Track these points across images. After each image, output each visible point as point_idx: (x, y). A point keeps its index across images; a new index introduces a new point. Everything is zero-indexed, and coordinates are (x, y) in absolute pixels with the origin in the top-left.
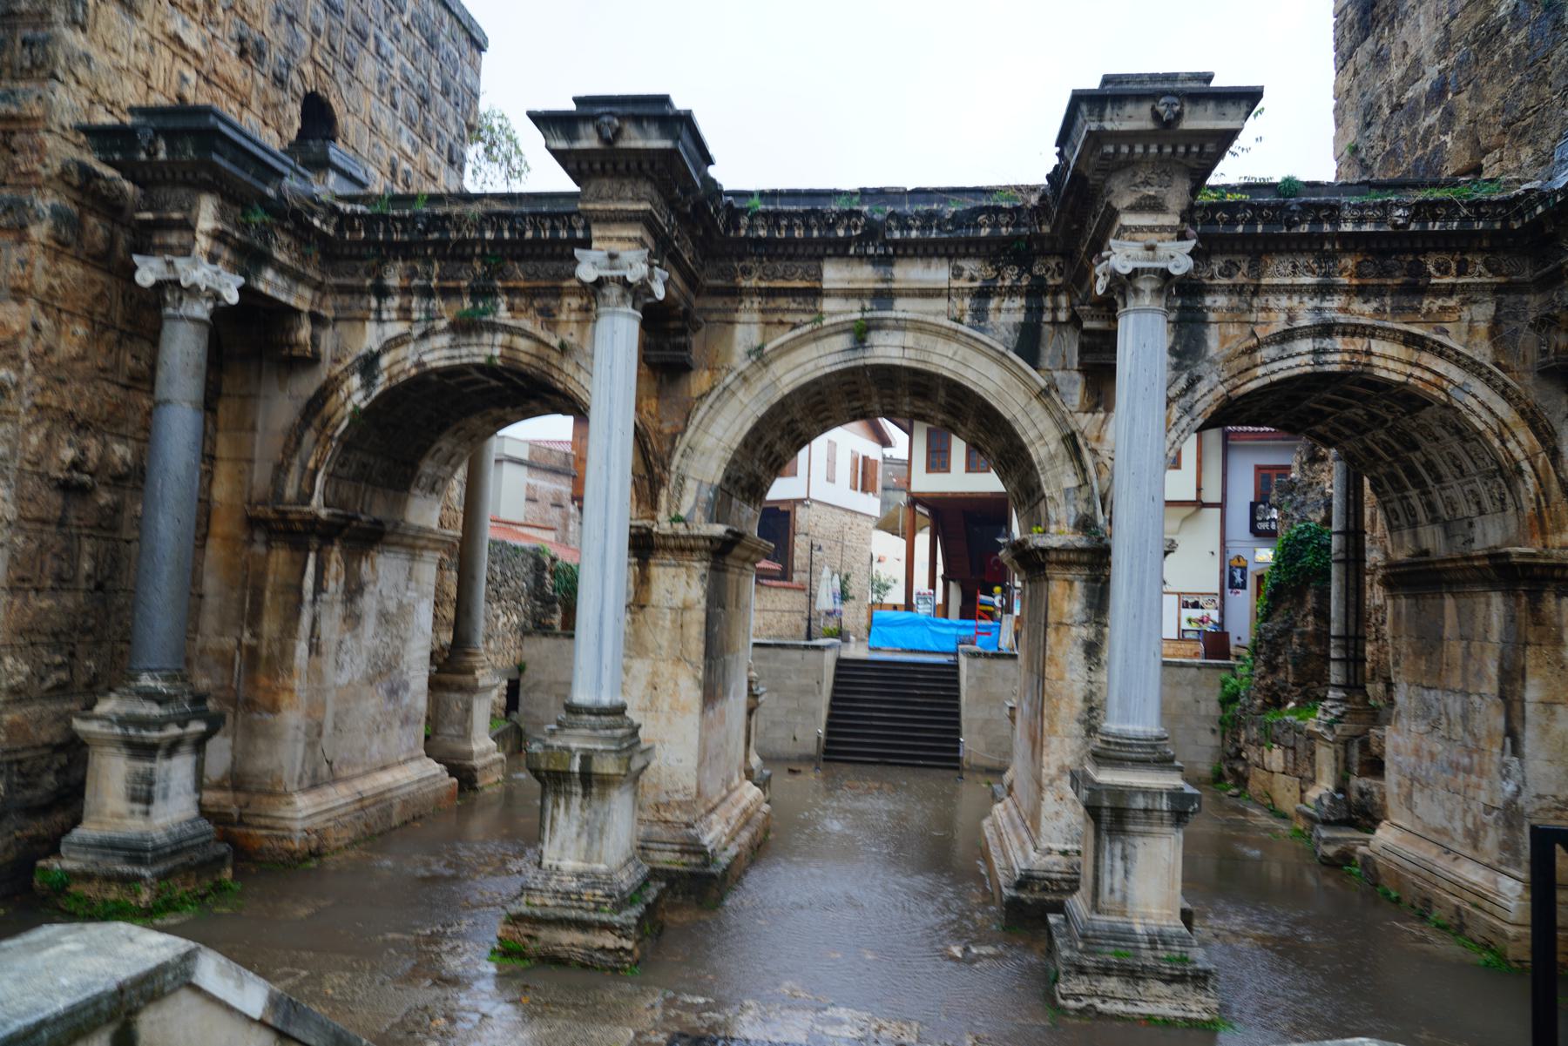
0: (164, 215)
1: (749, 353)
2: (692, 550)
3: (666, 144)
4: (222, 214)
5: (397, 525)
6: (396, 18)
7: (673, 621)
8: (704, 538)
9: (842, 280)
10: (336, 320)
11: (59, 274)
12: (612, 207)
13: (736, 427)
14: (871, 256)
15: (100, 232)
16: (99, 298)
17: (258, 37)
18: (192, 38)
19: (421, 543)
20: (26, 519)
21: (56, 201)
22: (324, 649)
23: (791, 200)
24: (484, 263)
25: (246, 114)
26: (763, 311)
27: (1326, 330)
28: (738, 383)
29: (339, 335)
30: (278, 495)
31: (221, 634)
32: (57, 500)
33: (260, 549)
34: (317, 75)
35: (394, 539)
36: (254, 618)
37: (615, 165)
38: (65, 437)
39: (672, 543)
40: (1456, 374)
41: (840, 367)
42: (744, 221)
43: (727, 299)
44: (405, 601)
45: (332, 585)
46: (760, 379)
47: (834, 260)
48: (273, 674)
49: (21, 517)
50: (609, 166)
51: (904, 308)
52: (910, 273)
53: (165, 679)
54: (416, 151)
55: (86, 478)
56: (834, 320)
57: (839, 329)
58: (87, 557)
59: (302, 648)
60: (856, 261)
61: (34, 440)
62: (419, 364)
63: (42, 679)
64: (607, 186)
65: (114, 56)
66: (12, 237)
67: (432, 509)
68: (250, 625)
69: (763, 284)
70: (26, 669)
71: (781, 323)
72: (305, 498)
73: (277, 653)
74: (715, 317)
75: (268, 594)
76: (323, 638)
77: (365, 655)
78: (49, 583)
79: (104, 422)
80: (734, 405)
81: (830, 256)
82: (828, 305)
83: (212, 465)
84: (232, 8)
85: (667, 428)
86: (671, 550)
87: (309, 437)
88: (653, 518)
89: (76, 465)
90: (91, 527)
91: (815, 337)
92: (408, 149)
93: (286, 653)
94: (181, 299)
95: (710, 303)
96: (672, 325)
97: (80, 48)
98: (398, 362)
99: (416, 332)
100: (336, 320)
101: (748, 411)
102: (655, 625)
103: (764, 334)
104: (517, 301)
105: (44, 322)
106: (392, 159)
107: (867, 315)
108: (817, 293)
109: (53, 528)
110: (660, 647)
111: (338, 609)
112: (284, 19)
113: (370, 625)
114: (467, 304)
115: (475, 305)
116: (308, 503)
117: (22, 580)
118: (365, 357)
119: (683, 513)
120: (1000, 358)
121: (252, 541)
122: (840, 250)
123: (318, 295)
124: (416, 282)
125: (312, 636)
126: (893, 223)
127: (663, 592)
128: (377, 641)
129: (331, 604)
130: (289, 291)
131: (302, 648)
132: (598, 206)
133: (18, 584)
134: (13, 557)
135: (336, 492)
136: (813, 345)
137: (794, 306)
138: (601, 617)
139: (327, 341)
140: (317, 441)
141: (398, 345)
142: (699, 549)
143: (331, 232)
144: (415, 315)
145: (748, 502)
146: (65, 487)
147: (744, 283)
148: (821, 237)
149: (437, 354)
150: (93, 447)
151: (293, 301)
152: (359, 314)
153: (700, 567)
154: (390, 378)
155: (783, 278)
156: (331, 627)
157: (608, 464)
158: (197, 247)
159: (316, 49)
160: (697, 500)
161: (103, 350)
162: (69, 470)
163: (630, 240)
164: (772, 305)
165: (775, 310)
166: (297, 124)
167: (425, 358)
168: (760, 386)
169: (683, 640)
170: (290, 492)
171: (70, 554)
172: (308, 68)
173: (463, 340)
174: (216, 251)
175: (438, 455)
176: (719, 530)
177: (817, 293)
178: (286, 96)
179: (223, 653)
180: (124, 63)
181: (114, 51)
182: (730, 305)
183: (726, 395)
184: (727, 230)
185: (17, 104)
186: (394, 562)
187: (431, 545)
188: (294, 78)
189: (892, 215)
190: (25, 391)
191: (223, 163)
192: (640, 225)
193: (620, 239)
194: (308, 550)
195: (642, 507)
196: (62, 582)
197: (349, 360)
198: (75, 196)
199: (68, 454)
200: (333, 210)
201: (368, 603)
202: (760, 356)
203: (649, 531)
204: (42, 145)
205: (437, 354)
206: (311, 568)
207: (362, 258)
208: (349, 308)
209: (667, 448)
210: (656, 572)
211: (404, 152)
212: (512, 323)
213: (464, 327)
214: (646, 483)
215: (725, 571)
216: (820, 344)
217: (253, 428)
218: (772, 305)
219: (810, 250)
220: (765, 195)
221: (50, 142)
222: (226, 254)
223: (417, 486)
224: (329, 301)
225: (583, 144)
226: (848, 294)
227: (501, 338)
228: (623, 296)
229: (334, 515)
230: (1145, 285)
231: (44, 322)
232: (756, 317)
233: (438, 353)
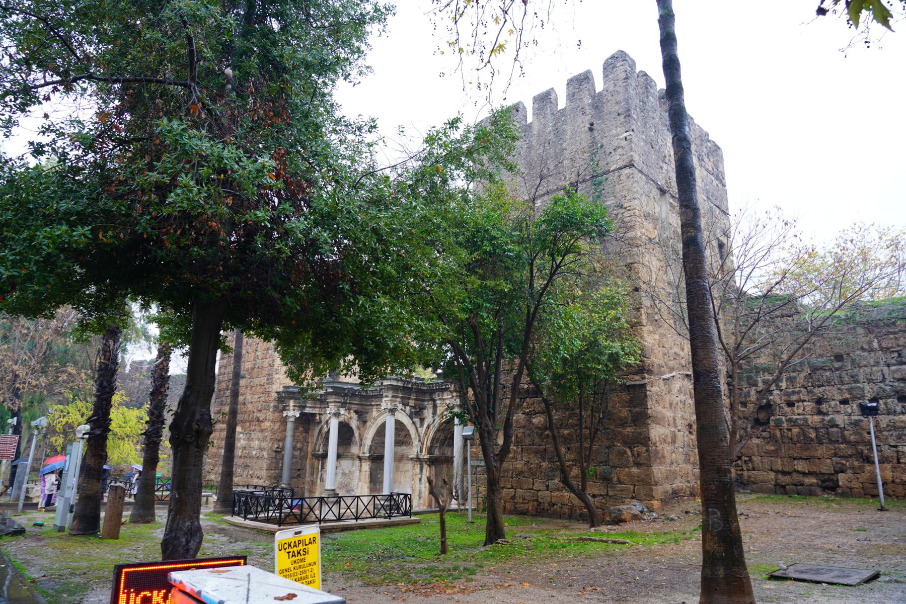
4: (295, 402)
30: (315, 450)
32: (274, 454)
36: (312, 474)
59: (319, 480)
72: (319, 451)
89: (278, 448)
131: (319, 480)
150: (281, 444)
196: (276, 468)
199: (276, 446)
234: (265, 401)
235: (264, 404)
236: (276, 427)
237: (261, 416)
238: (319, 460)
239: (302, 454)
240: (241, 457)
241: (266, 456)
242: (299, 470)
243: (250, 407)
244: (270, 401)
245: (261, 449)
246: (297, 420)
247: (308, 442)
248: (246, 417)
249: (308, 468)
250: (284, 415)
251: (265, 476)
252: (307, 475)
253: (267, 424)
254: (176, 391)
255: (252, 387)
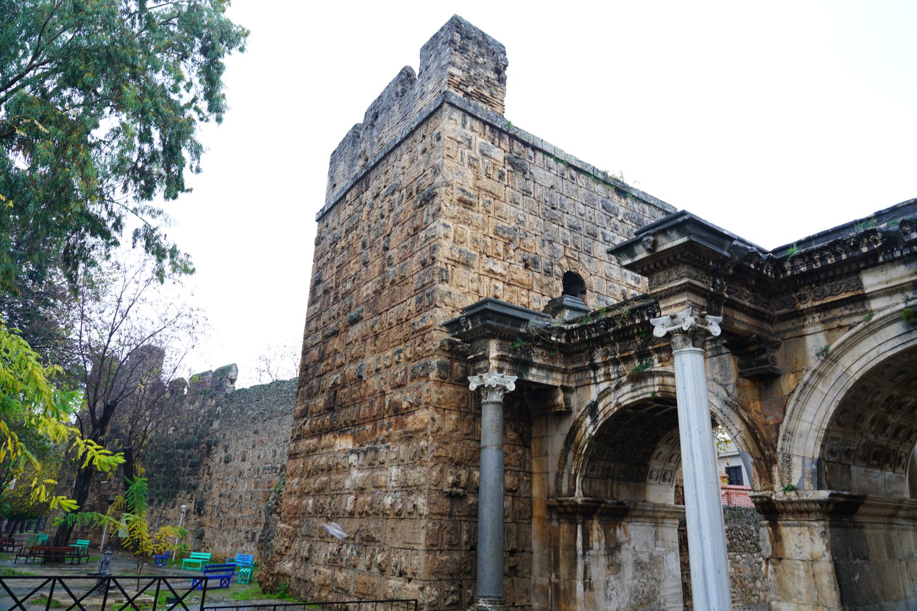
0: (477, 355)
1: (818, 355)
2: (808, 512)
3: (685, 239)
4: (501, 347)
5: (636, 504)
6: (614, 220)
7: (807, 572)
8: (815, 502)
9: (880, 283)
10: (577, 387)
11: (442, 393)
12: (666, 288)
13: (822, 412)
14: (899, 259)
15: (460, 368)
16: (462, 400)
17: (533, 256)
18: (498, 269)
19: (660, 514)
20: (434, 514)
21: (439, 359)
22: (595, 586)
23: (825, 238)
24: (641, 338)
25: (531, 294)
26: (823, 322)
28: (814, 379)
29: (579, 395)
30: (558, 491)
31: (542, 576)
32: (447, 503)
33: (555, 524)
34: (569, 263)
35: (637, 513)
36: (555, 566)
37: (661, 262)
38: (449, 470)
39: (790, 507)
41: (899, 349)
42: (787, 265)
43: (794, 321)
44: (655, 554)
45: (596, 545)
46: (833, 372)
47: (870, 270)
48: (568, 603)
49: (431, 513)
50: (658, 264)
53: (491, 602)
54: (638, 283)
55: (460, 490)
56: (882, 314)
57: (890, 320)
58: (465, 533)
60: (888, 266)
61: (434, 474)
62: (618, 404)
63: (445, 599)
64: (662, 276)
65: (462, 289)
66: (425, 380)
67: (667, 491)
68: (555, 571)
69: (817, 303)
70: (436, 593)
71: (840, 327)
72: (572, 492)
73: (568, 589)
74: (789, 335)
75: (561, 551)
76: (593, 579)
77: (627, 590)
78: (446, 547)
79: (469, 461)
80: (816, 397)
81: (865, 268)
82: (875, 304)
83: (531, 478)
84: (518, 248)
85: (771, 420)
86: (793, 513)
87: (570, 455)
88: (772, 489)
89: (455, 484)
90: (465, 516)
91: (871, 330)
92: (633, 283)
93: (572, 588)
94: (487, 393)
95: (782, 327)
96: (752, 349)
97: (446, 290)
98: (607, 405)
99: (613, 386)
100: (577, 387)
101: (829, 398)
102: (793, 574)
103: (827, 338)
104: (663, 355)
105: (436, 416)
106: (623, 291)
107: (910, 303)
108: (863, 298)
109: (446, 518)
110: (800, 593)
111: (603, 560)
112: (547, 243)
113: (628, 571)
114: (637, 363)
115: (641, 362)
116: (573, 496)
117: (432, 545)
118: (590, 405)
119: (795, 483)
121: (550, 520)
122: (871, 262)
123: (566, 376)
124: (609, 357)
125: (585, 578)
126: (907, 229)
127: (794, 548)
128: (636, 582)
129: (597, 557)
130: (547, 377)
132: (658, 290)
133: (430, 548)
134: (427, 534)
135: (591, 487)
136: (871, 337)
137: (847, 312)
138: (704, 569)
139: (574, 399)
140: (574, 458)
141: (606, 396)
142: (815, 511)
143: (563, 341)
144: (613, 377)
145: (881, 467)
146: (451, 496)
147: (802, 307)
148: (849, 258)
149: (626, 397)
150: (464, 474)
151: (550, 382)
152: (586, 382)
153: (818, 526)
154: (605, 416)
155: (830, 295)
156: (598, 571)
157: (692, 455)
158: (491, 367)
159: (567, 250)
160: (803, 472)
161: (466, 425)
162: (452, 487)
163: (682, 304)
164: (829, 316)
165: (833, 319)
166: (561, 290)
167: (621, 400)
168: (834, 378)
169: (817, 587)
170: (565, 489)
171: (456, 531)
172: (564, 262)
173: (638, 386)
174: (501, 366)
175: (661, 457)
176: (824, 494)
177: (863, 298)
178: (551, 279)
179: (543, 587)
180: (467, 290)
181: (462, 286)
182: (798, 324)
183: (808, 389)
184: (777, 275)
185: (425, 322)
186: (642, 528)
187: (668, 515)
188: (557, 269)
189: (903, 223)
190: (430, 450)
191: (494, 323)
192: (686, 293)
193: (676, 305)
194: (577, 524)
195: (763, 479)
196: (453, 546)
197: (583, 409)
198: (448, 355)
199: (451, 479)
200: (561, 330)
201: (625, 556)
202: (829, 357)
203: (770, 499)
204: (433, 336)
205: (626, 397)
206: (579, 535)
207: (581, 351)
208: (582, 380)
209: (774, 435)
210: (784, 531)
211: (630, 285)
212: (661, 369)
213: (638, 378)
214: (763, 463)
215: (861, 527)
216: (876, 335)
217: (547, 455)
218: (829, 316)
219: (846, 269)
220: (800, 243)
221: (435, 334)
222: (507, 366)
223: (651, 478)
224: (572, 378)
225: (639, 257)
226: (890, 292)
227: (657, 380)
228: (684, 340)
229: (586, 501)
231: (436, 416)
232: (820, 328)
233: (626, 396)
234: (417, 357)
235: (410, 365)
236: (449, 426)
237: (404, 398)
238: (573, 523)
239: (519, 505)
240: (352, 514)
241: (424, 510)
242: (513, 552)
243: (373, 383)
244: (429, 353)
245: (407, 489)
246: (510, 400)
247: (531, 473)
248: (364, 409)
249: (535, 545)
250: (473, 386)
251: (421, 572)
252: (536, 568)
253: (423, 415)
254: (250, 412)
255: (376, 336)
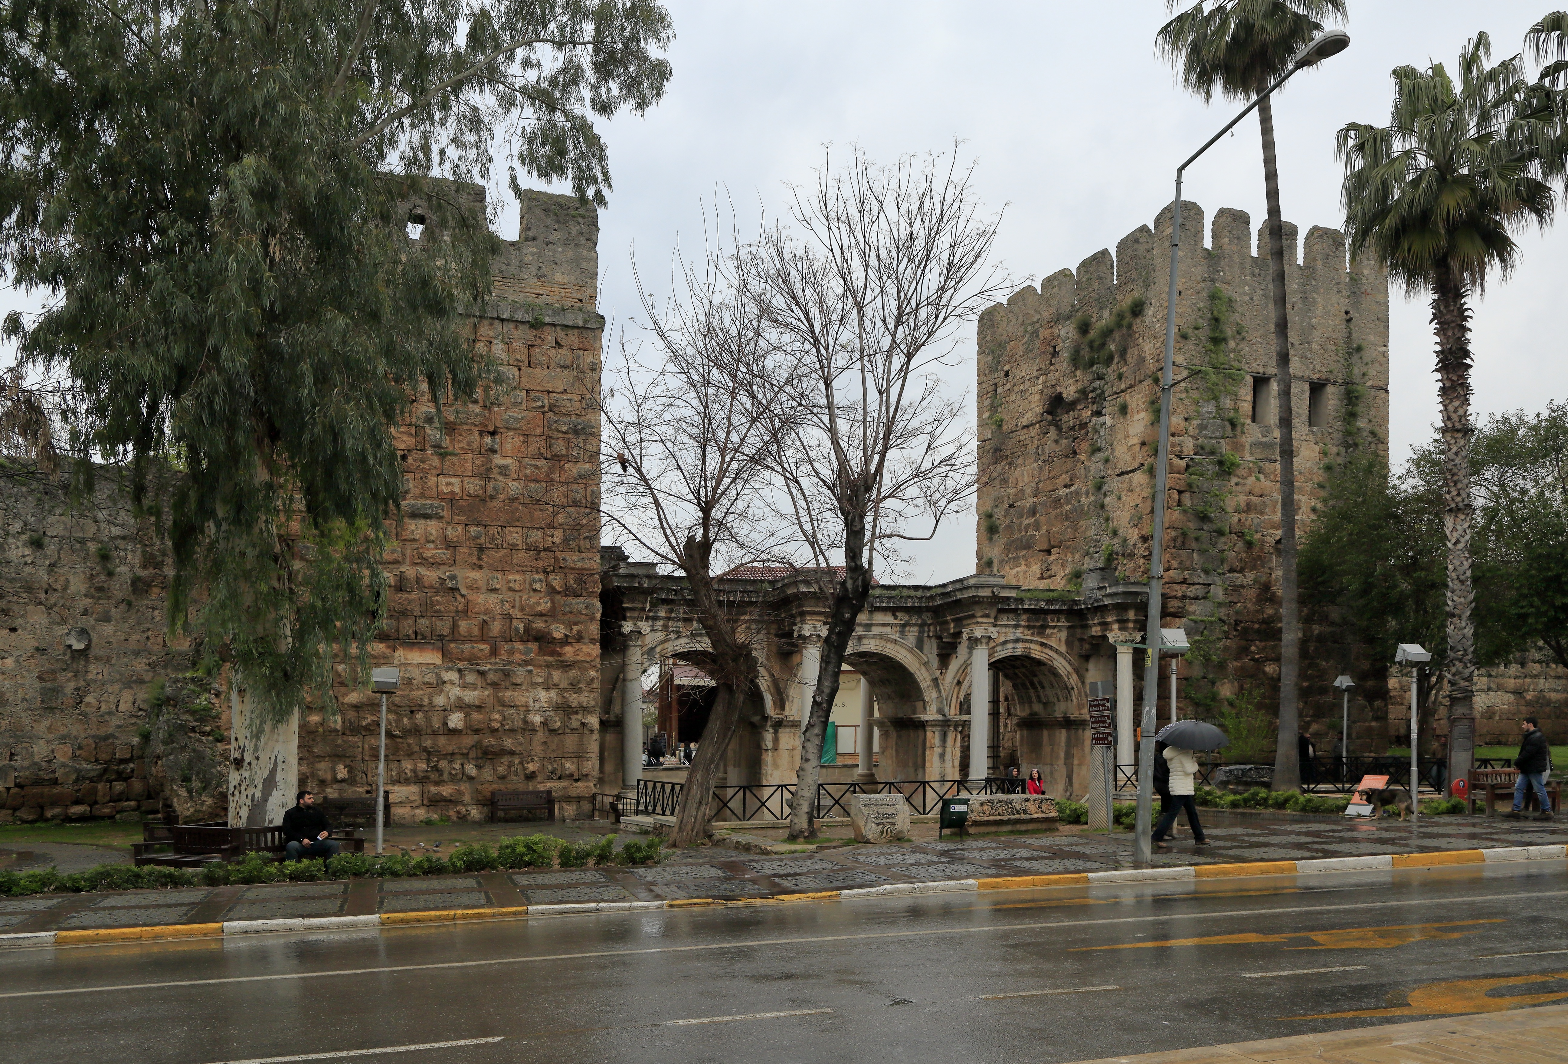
27: (1017, 640)
40: (1055, 656)
51: (876, 630)
52: (879, 618)
120: (911, 651)
230: (984, 641)
